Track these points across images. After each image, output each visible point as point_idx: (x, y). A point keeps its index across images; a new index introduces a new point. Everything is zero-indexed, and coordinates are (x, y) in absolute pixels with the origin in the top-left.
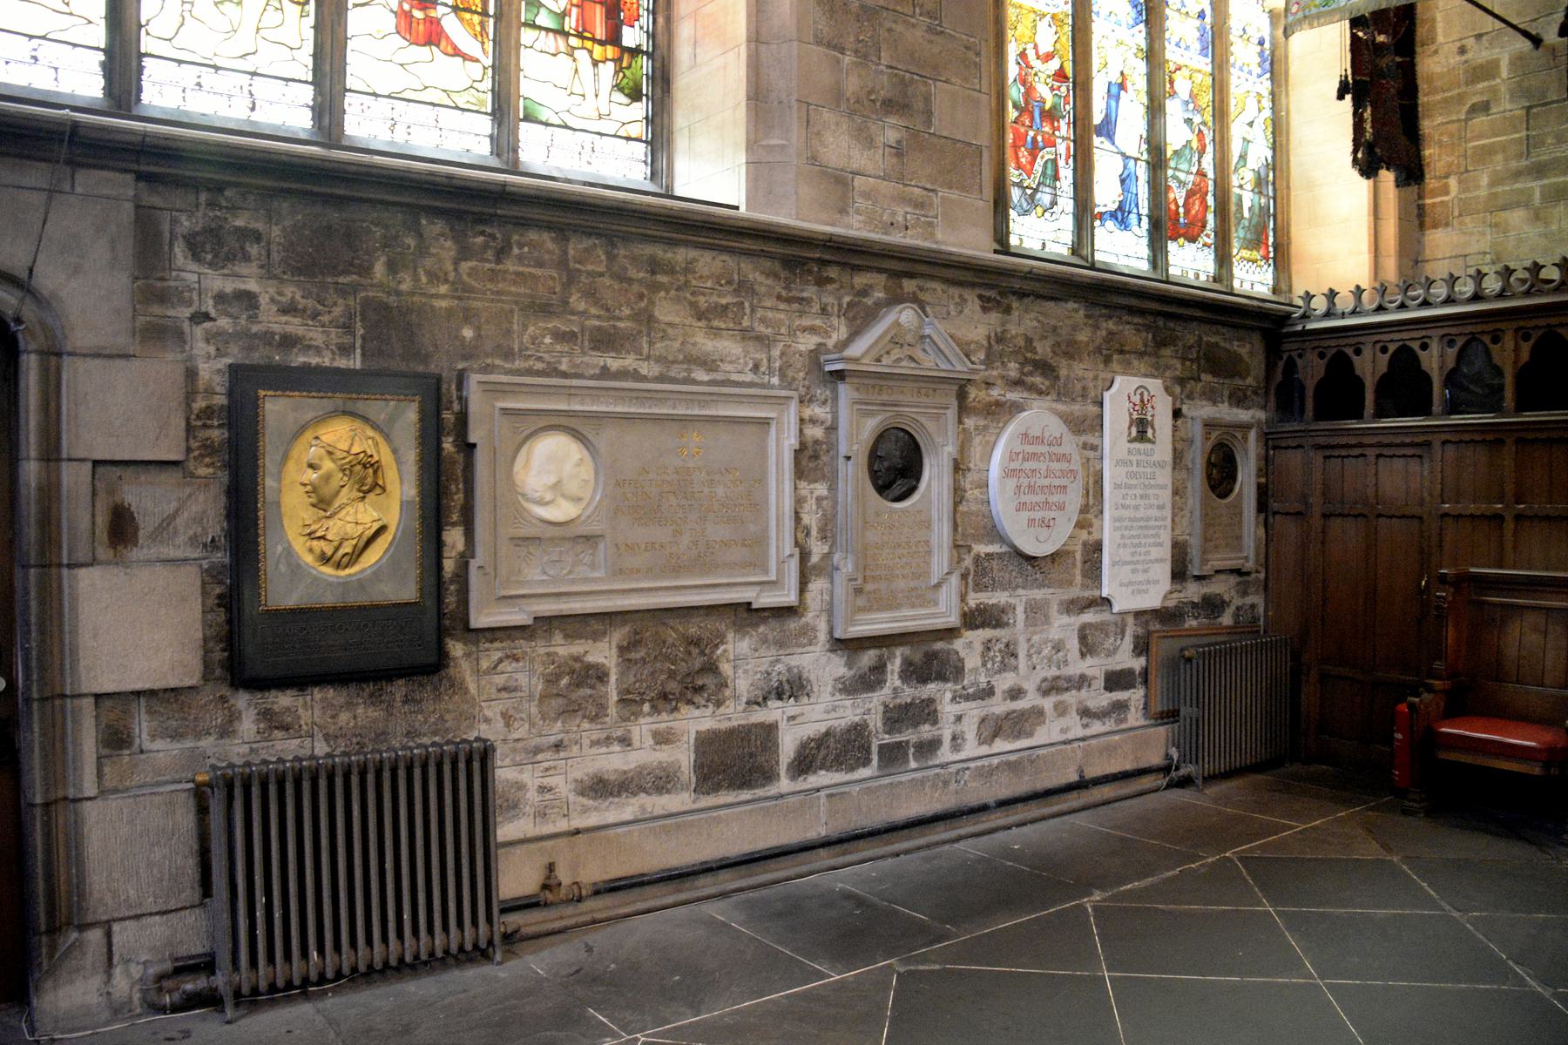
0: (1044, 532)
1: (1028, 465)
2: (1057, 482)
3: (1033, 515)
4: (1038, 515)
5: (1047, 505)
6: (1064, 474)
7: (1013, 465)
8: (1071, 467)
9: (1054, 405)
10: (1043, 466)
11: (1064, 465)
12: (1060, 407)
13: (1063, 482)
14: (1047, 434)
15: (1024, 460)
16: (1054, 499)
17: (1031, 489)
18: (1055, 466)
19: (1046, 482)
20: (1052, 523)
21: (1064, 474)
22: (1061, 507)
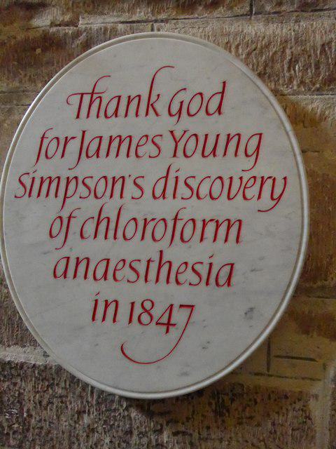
0: (150, 340)
1: (93, 168)
2: (202, 210)
3: (108, 290)
4: (127, 292)
5: (164, 269)
6: (228, 188)
7: (46, 169)
8: (262, 170)
9: (234, 27)
10: (151, 171)
11: (234, 166)
12: (255, 29)
13: (224, 209)
14: (165, 88)
15: (83, 152)
16: (197, 252)
17: (105, 225)
18: (195, 167)
19: (165, 208)
20: (179, 317)
21: (228, 188)
22: (221, 277)
